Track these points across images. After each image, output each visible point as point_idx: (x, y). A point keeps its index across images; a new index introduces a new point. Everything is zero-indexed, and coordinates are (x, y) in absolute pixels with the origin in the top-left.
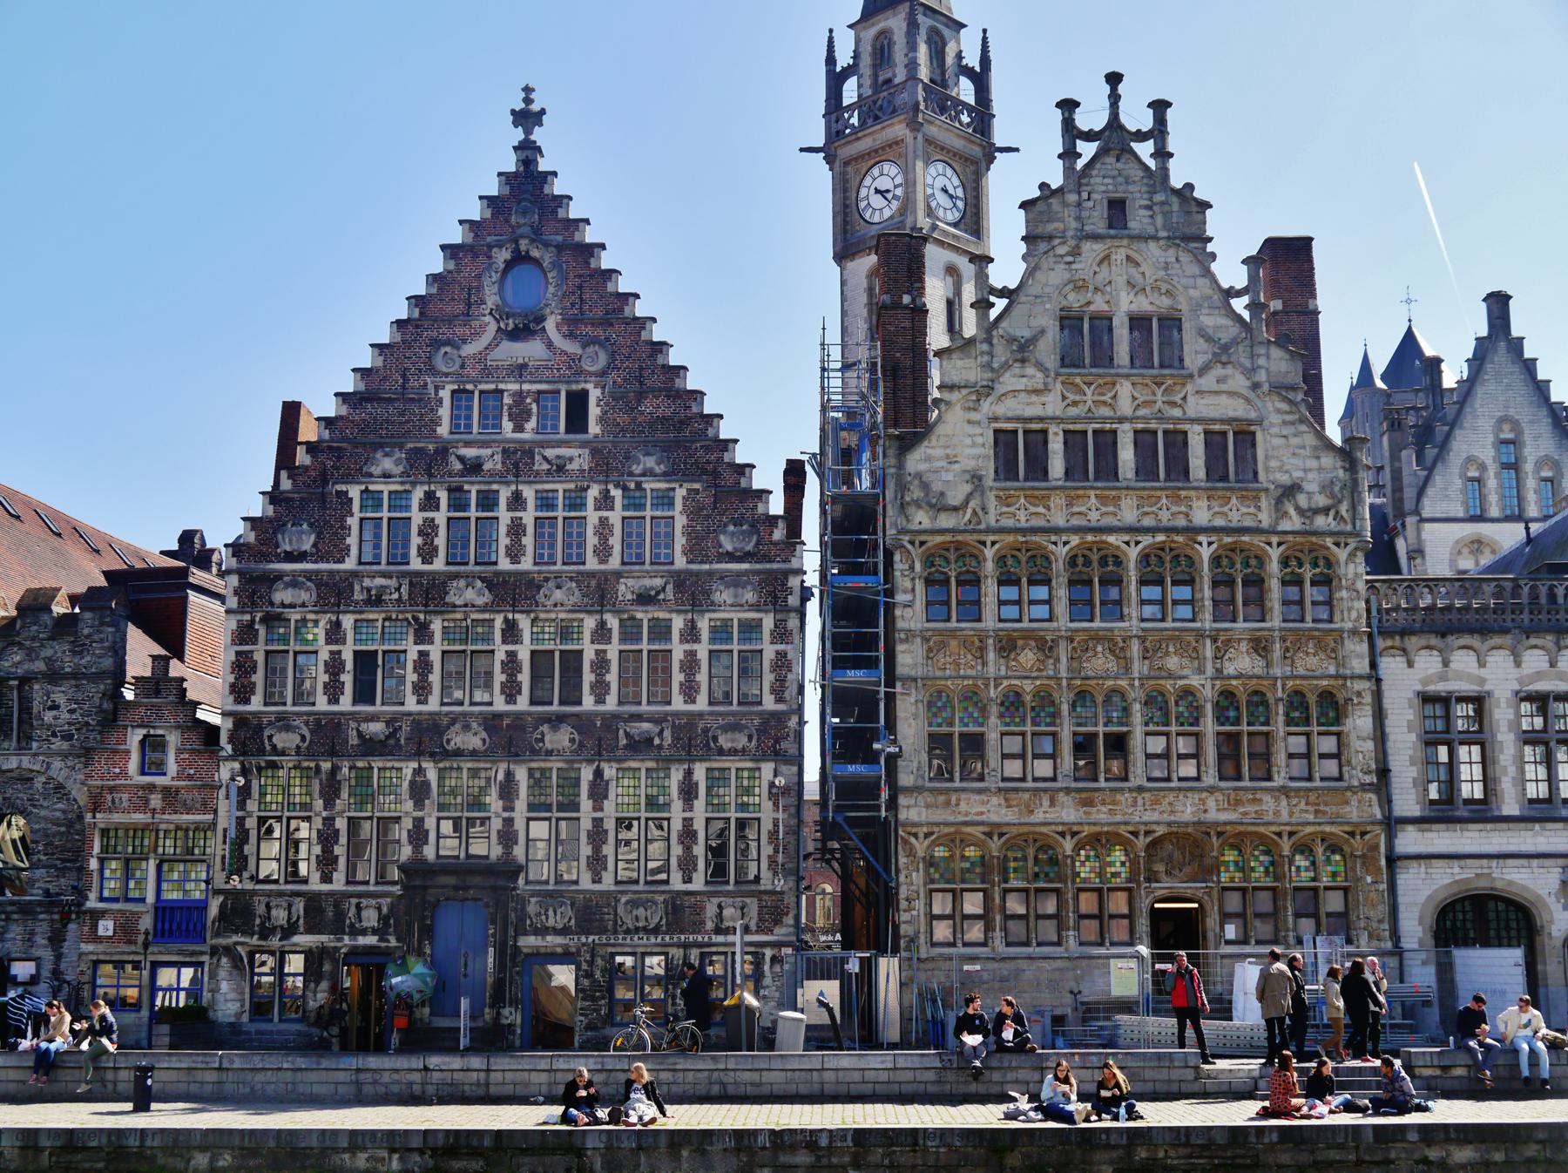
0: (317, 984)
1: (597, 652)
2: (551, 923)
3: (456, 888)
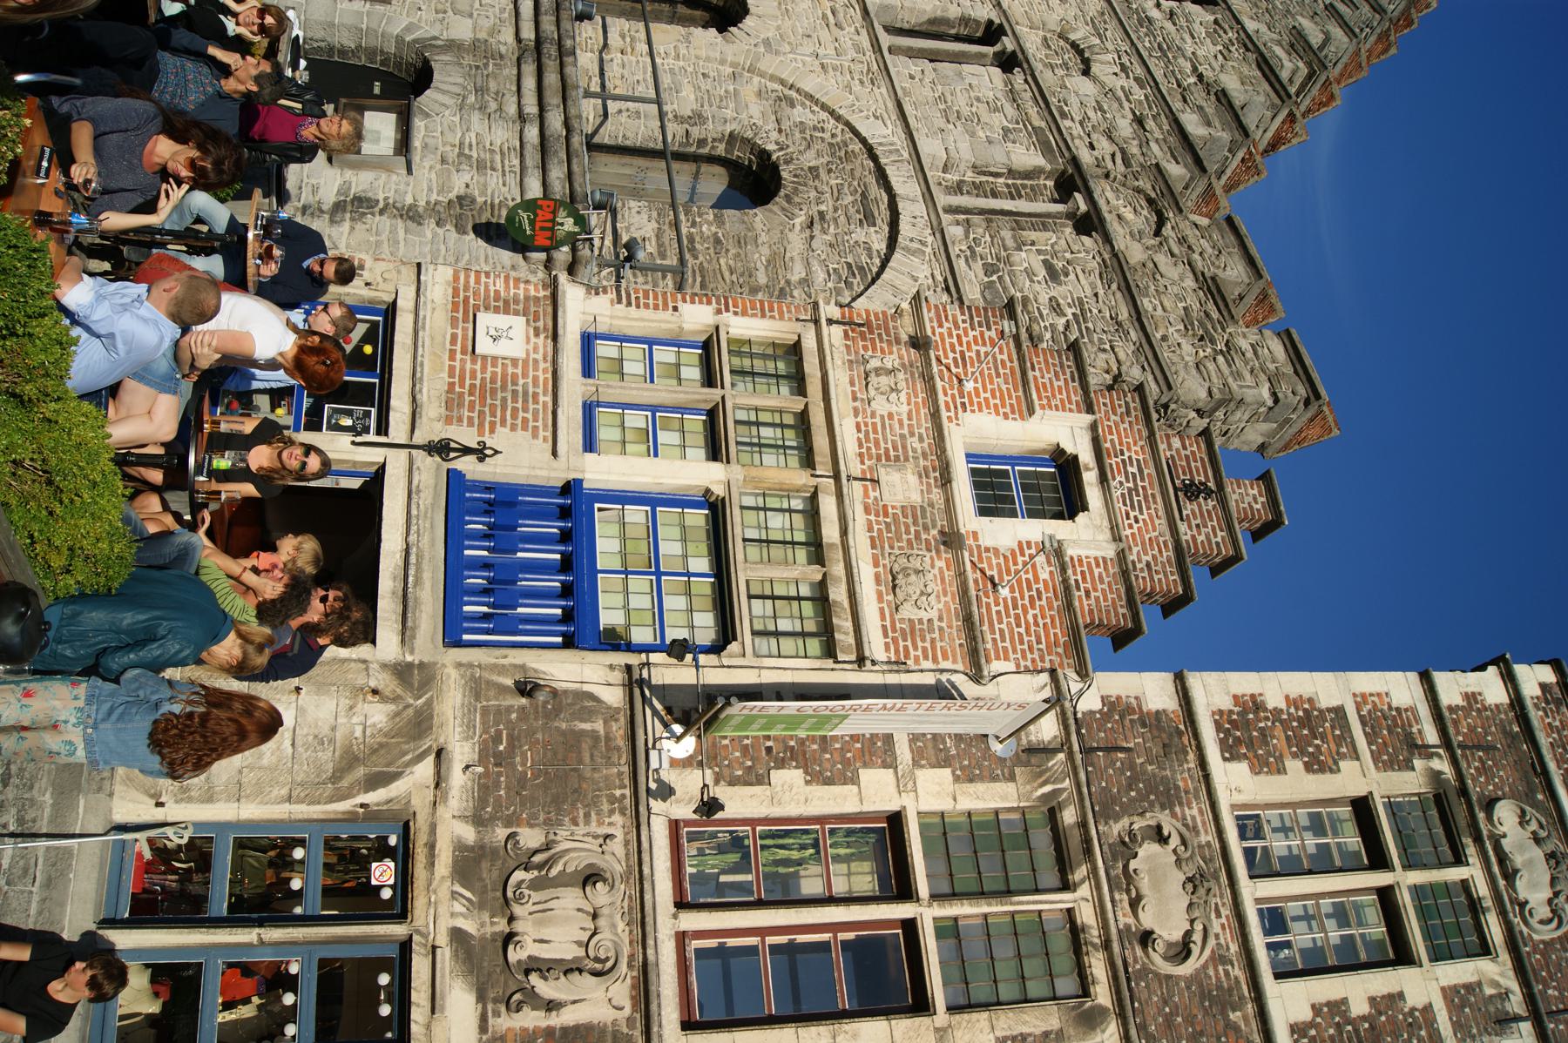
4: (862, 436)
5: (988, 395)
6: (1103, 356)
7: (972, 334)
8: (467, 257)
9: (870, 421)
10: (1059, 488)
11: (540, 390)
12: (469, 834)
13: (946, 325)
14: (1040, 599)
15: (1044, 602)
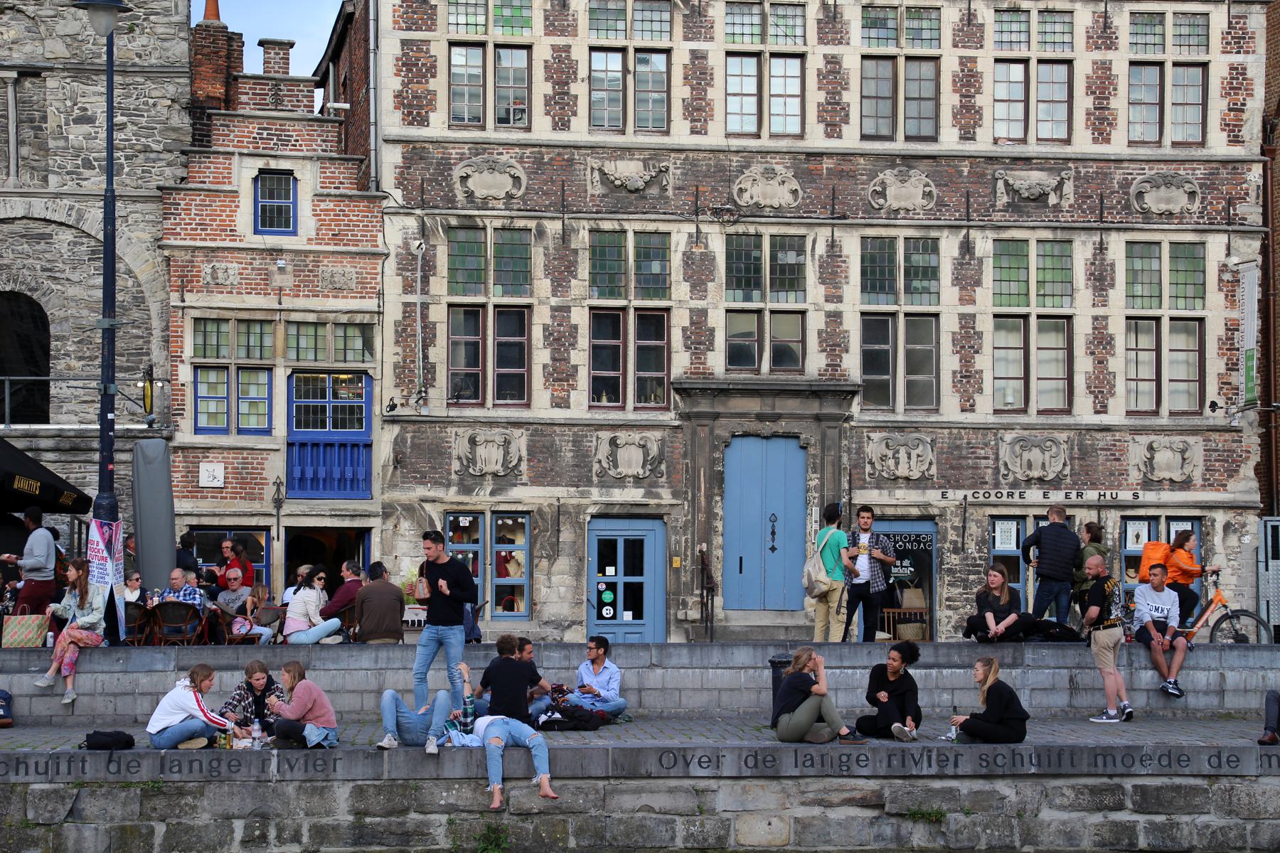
0: (552, 558)
1: (963, 61)
2: (902, 471)
3: (760, 417)
6: (159, 108)
10: (275, 183)
12: (453, 489)
13: (178, 230)
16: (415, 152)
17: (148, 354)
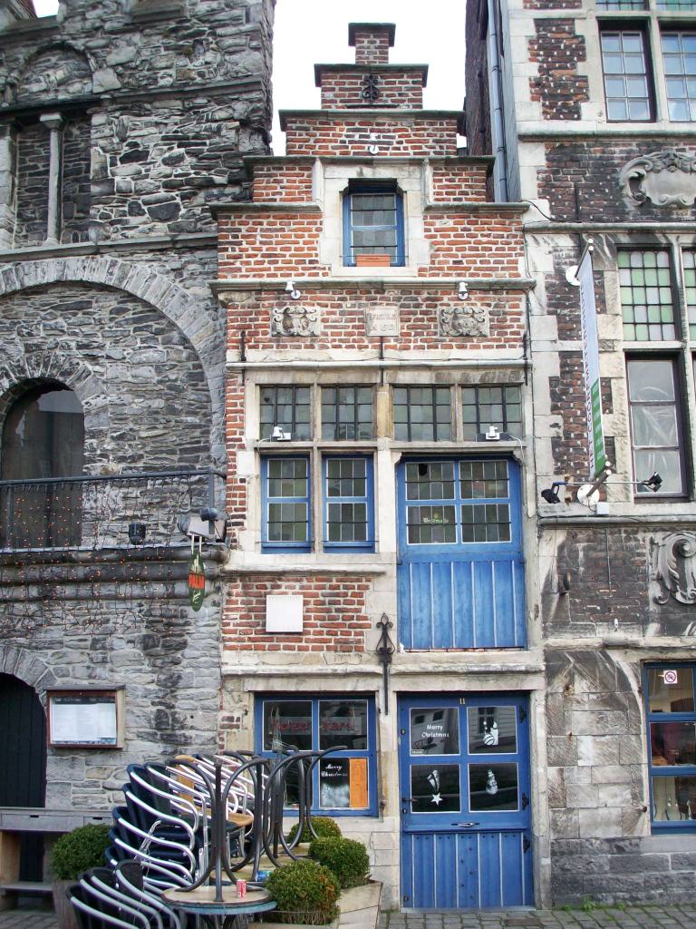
4: (344, 345)
5: (301, 240)
6: (224, 132)
7: (244, 245)
8: (210, 641)
9: (330, 338)
11: (328, 584)
12: (653, 627)
13: (238, 264)
14: (470, 230)
15: (472, 227)
16: (563, 150)
17: (207, 449)
